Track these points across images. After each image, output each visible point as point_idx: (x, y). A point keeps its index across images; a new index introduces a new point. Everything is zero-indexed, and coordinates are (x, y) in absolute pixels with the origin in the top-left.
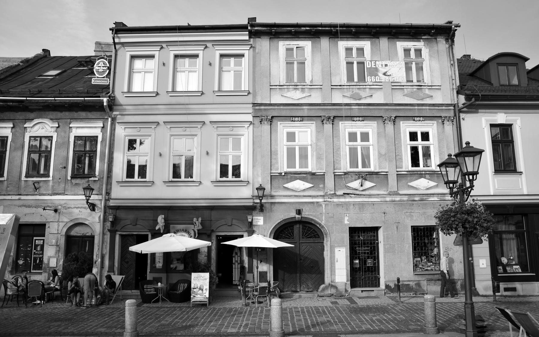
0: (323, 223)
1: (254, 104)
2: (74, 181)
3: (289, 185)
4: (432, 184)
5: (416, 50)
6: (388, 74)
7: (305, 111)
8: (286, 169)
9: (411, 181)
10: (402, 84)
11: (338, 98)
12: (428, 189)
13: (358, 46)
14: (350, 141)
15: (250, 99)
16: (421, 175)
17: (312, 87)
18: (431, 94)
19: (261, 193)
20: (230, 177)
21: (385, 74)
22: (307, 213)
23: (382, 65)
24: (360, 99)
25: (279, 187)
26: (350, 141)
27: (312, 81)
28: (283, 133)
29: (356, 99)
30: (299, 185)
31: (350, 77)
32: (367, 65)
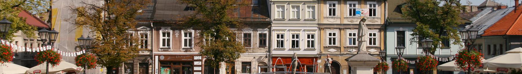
0: (340, 62)
1: (318, 24)
2: (260, 48)
3: (329, 50)
4: (376, 50)
5: (374, 5)
6: (363, 13)
7: (335, 27)
8: (329, 45)
9: (368, 50)
10: (368, 17)
11: (346, 22)
12: (374, 52)
13: (354, 3)
14: (349, 36)
15: (316, 22)
16: (372, 48)
17: (337, 18)
18: (377, 20)
19: (321, 53)
20: (310, 48)
21: (362, 13)
22: (335, 59)
23: (361, 10)
24: (353, 22)
25: (326, 51)
26: (349, 36)
27: (337, 16)
28: (328, 33)
29: (352, 22)
30: (332, 50)
31: (350, 14)
32: (356, 10)
